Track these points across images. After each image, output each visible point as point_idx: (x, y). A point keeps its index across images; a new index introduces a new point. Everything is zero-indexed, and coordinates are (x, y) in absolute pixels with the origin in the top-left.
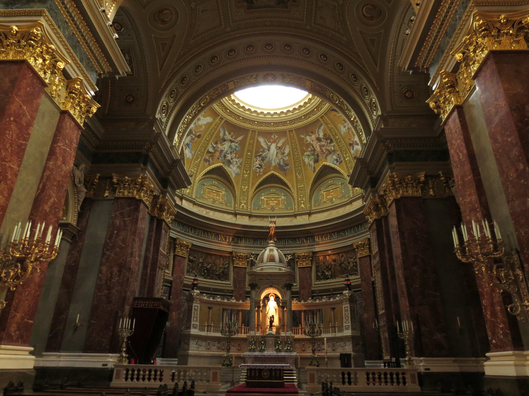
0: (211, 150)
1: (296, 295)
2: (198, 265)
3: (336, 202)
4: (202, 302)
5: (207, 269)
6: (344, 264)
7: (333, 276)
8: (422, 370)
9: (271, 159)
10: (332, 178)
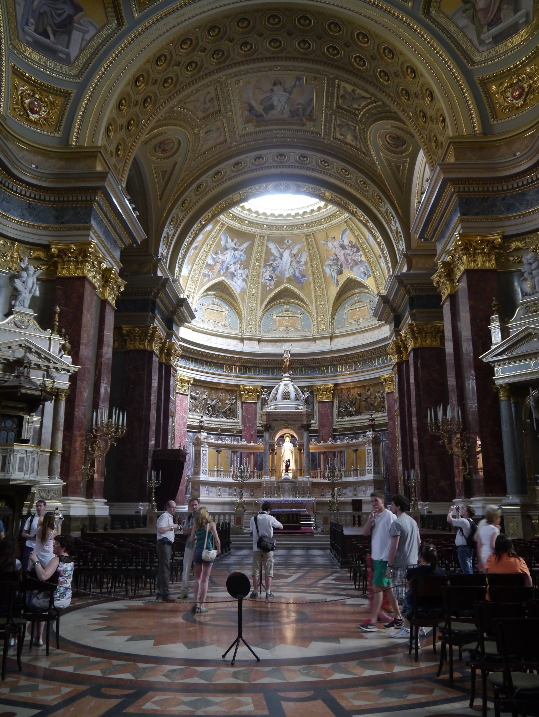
0: (210, 262)
1: (315, 434)
2: (202, 401)
3: (364, 324)
4: (211, 445)
5: (211, 406)
6: (371, 399)
7: (358, 412)
8: (426, 513)
9: (284, 269)
10: (359, 293)
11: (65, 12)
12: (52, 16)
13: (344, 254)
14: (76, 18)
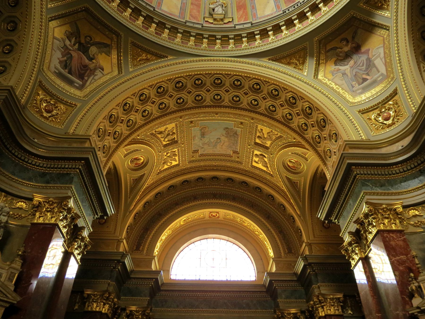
11: (363, 60)
12: (361, 70)
14: (370, 56)
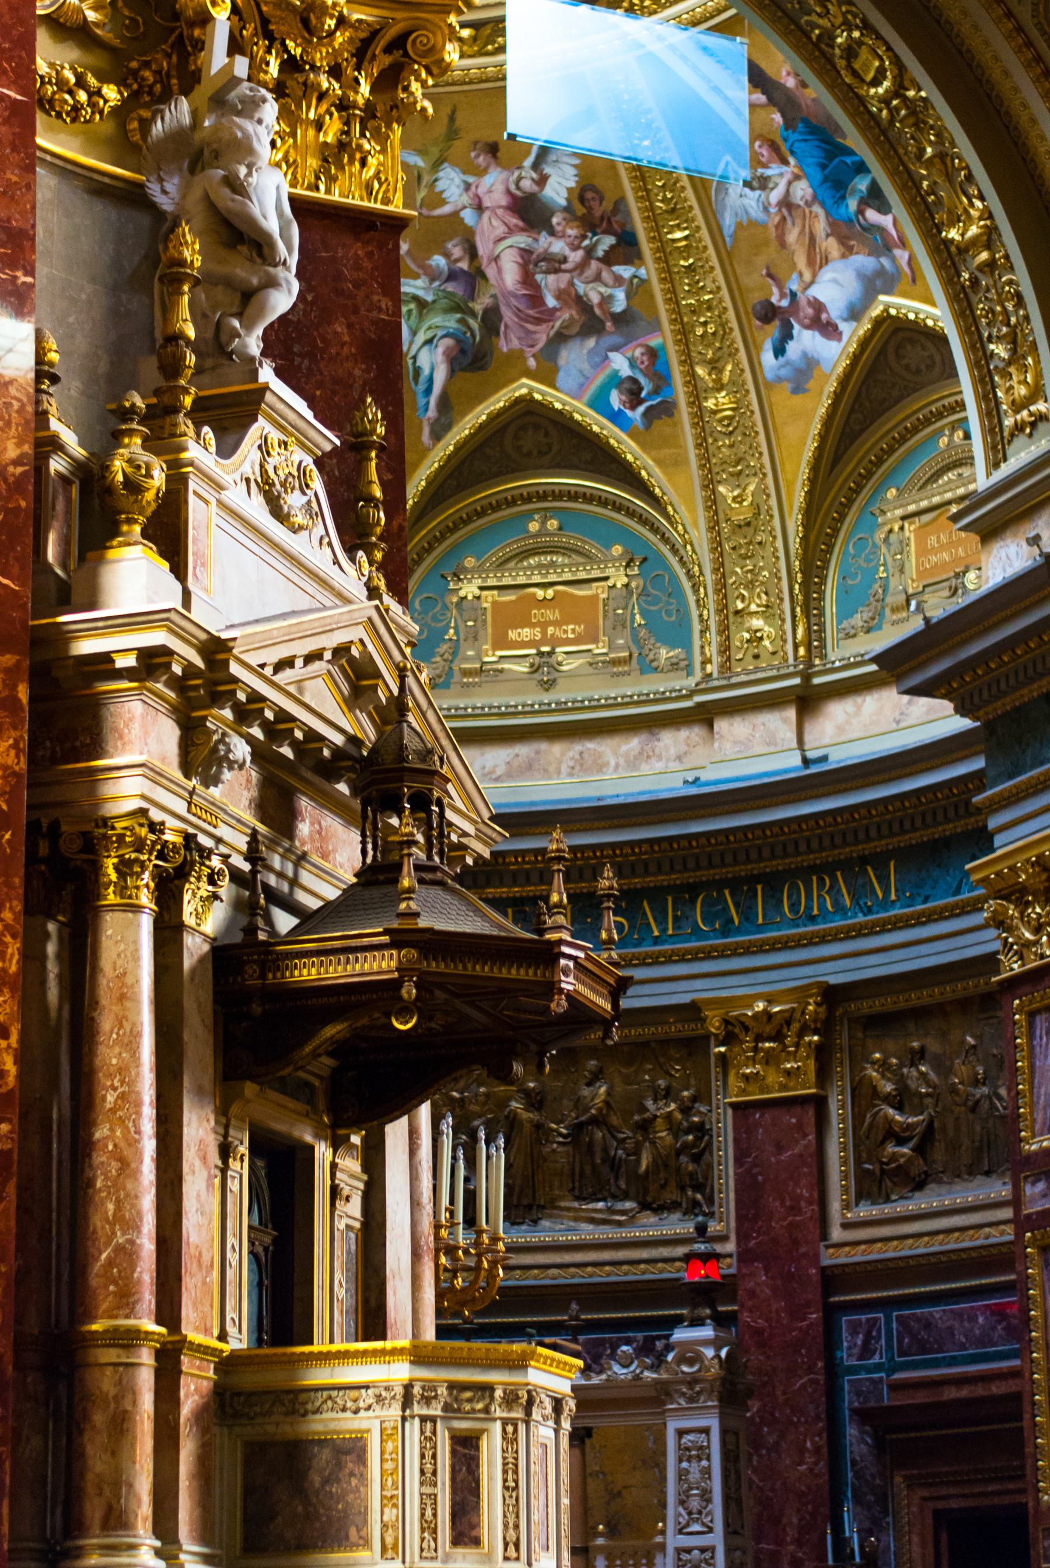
6: (612, 1130)
13: (526, 253)
